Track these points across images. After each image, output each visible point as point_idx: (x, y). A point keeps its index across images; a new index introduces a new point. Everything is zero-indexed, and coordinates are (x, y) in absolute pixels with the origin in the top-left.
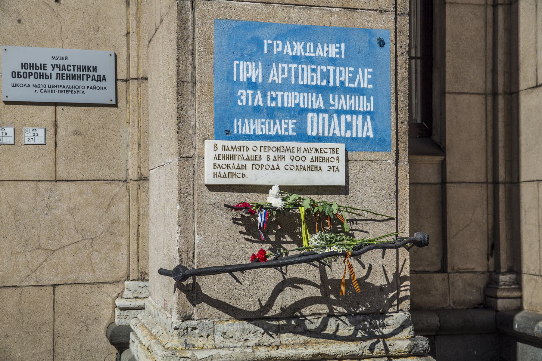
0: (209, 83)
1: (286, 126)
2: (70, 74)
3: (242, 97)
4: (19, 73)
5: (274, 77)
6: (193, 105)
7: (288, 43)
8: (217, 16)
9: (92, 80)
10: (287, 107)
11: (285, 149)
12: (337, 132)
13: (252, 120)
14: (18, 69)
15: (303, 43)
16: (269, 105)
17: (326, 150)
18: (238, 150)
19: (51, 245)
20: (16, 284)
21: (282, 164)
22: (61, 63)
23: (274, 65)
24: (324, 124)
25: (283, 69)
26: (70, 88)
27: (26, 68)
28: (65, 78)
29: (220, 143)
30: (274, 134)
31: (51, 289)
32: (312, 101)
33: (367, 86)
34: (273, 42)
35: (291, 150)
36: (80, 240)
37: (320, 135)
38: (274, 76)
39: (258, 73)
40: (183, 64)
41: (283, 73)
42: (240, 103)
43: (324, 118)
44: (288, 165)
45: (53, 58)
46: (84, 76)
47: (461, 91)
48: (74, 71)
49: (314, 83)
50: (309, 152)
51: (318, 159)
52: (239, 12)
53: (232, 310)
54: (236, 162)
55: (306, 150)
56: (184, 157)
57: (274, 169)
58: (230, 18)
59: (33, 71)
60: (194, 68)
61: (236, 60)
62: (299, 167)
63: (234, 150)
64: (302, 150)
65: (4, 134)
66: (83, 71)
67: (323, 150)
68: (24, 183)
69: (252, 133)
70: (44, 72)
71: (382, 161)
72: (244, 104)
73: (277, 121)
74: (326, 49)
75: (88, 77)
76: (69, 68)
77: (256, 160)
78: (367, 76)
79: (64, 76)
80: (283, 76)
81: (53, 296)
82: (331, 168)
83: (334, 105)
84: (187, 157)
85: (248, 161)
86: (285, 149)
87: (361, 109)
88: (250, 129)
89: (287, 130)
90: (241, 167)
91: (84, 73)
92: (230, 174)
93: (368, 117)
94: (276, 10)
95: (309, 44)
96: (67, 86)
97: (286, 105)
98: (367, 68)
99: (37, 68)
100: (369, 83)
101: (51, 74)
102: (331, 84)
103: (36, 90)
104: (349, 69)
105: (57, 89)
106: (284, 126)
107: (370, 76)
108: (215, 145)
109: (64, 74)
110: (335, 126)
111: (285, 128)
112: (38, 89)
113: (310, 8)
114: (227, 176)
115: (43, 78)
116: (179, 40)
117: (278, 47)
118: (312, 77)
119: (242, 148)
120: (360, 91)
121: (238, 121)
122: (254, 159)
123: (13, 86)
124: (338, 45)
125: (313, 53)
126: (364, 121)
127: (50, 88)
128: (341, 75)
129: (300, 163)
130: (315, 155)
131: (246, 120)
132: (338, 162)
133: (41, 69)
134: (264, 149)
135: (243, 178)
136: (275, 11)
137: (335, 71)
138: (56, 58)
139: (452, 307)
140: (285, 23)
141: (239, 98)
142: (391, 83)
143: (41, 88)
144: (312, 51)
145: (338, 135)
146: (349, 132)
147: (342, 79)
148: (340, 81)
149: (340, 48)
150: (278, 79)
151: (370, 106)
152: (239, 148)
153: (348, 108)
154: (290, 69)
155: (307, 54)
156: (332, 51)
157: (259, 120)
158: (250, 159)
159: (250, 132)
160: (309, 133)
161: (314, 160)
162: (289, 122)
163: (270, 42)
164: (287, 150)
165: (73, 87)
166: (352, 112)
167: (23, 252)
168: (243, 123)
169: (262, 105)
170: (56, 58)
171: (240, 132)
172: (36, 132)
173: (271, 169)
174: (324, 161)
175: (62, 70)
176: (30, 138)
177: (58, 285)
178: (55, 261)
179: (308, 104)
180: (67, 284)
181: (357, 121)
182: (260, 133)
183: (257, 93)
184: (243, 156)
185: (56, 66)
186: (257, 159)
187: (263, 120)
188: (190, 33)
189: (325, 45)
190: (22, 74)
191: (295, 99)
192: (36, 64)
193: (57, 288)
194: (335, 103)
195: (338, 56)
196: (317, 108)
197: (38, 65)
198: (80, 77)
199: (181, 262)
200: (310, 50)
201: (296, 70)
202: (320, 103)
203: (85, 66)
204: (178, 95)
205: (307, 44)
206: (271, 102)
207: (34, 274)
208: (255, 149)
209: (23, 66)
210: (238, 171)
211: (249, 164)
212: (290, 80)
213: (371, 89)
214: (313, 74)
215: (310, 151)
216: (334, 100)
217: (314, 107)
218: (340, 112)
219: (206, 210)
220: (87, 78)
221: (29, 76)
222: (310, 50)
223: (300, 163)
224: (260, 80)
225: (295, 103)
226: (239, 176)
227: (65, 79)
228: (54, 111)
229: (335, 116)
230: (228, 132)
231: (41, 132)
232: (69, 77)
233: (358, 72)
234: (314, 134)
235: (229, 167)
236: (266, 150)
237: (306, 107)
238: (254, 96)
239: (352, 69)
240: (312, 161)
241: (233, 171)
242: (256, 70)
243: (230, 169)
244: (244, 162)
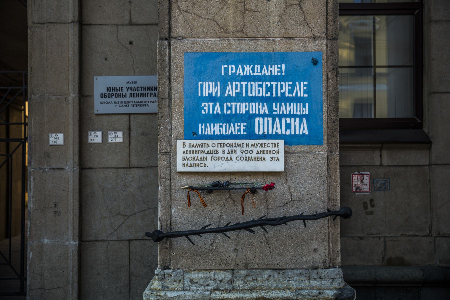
0: (180, 99)
1: (239, 128)
2: (138, 93)
4: (106, 95)
5: (229, 92)
6: (170, 115)
7: (240, 66)
8: (186, 50)
9: (154, 97)
10: (240, 113)
11: (236, 145)
12: (279, 131)
13: (212, 124)
14: (105, 91)
15: (252, 66)
16: (225, 112)
17: (269, 145)
18: (201, 146)
19: (127, 212)
20: (104, 239)
21: (234, 156)
22: (132, 85)
23: (229, 83)
24: (268, 125)
25: (236, 86)
26: (139, 102)
27: (110, 91)
28: (136, 96)
29: (187, 142)
30: (230, 134)
31: (127, 243)
32: (259, 109)
33: (303, 96)
34: (228, 67)
35: (242, 146)
36: (146, 209)
37: (265, 133)
38: (229, 91)
39: (217, 90)
40: (162, 86)
41: (236, 88)
42: (203, 112)
43: (268, 121)
44: (239, 157)
45: (128, 83)
46: (148, 94)
47: (445, 91)
48: (141, 91)
49: (260, 95)
50: (255, 147)
51: (262, 152)
52: (202, 46)
53: (198, 263)
54: (199, 156)
55: (253, 145)
56: (163, 153)
57: (228, 160)
58: (196, 51)
59: (114, 93)
60: (170, 88)
61: (200, 81)
62: (247, 158)
63: (198, 147)
64: (250, 146)
65: (96, 136)
66: (148, 91)
67: (266, 145)
68: (109, 170)
70: (122, 92)
72: (207, 112)
73: (232, 124)
74: (270, 69)
75: (151, 94)
76: (138, 89)
77: (214, 153)
78: (303, 88)
79: (135, 95)
80: (237, 91)
81: (128, 247)
82: (273, 159)
83: (276, 111)
84: (165, 152)
85: (208, 154)
86: (236, 145)
87: (298, 113)
88: (211, 131)
89: (239, 130)
90: (203, 159)
91: (148, 92)
92: (195, 164)
93: (304, 119)
94: (231, 43)
95: (256, 66)
96: (137, 102)
97: (238, 112)
98: (303, 82)
99: (117, 90)
100: (304, 93)
101: (126, 94)
102: (274, 95)
103: (116, 106)
104: (288, 83)
105: (130, 104)
106: (237, 128)
108: (184, 144)
109: (135, 93)
110: (277, 127)
111: (238, 129)
112: (118, 105)
113: (257, 40)
114: (193, 165)
115: (121, 97)
116: (159, 69)
117: (232, 69)
118: (259, 91)
119: (204, 145)
120: (297, 100)
121: (202, 126)
122: (213, 153)
123: (102, 103)
124: (279, 66)
125: (259, 73)
127: (126, 103)
128: (282, 88)
129: (249, 155)
130: (259, 149)
131: (208, 124)
132: (279, 154)
133: (119, 91)
134: (221, 145)
135: (204, 166)
136: (230, 43)
137: (277, 86)
138: (130, 83)
139: (438, 265)
140: (237, 52)
141: (203, 108)
142: (323, 92)
143: (120, 104)
144: (259, 71)
145: (280, 133)
146: (288, 131)
147: (283, 91)
148: (281, 92)
149: (281, 68)
151: (306, 111)
152: (202, 145)
153: (288, 113)
154: (241, 86)
155: (255, 74)
156: (275, 70)
157: (218, 124)
158: (210, 153)
159: (211, 133)
160: (257, 132)
161: (259, 153)
162: (241, 124)
163: (226, 66)
164: (238, 145)
165: (141, 102)
167: (109, 217)
168: (206, 127)
169: (220, 113)
170: (130, 83)
172: (116, 135)
173: (226, 160)
174: (267, 153)
175: (133, 91)
176: (113, 138)
177: (132, 240)
178: (130, 223)
179: (256, 111)
180: (138, 240)
181: (295, 123)
182: (219, 133)
183: (216, 104)
184: (204, 151)
185: (129, 88)
186: (215, 153)
187: (221, 124)
188: (167, 63)
189: (269, 66)
190: (107, 95)
191: (246, 107)
192: (116, 88)
193: (131, 242)
194: (277, 109)
195: (279, 74)
196: (263, 113)
197: (118, 88)
198: (145, 95)
199: (162, 227)
201: (247, 86)
202: (265, 110)
203: (149, 87)
204: (159, 108)
205: (254, 66)
206: (227, 111)
207: (116, 232)
208: (214, 145)
209: (108, 89)
210: (201, 162)
211: (209, 156)
213: (306, 97)
214: (259, 88)
215: (256, 146)
216: (276, 107)
217: (261, 113)
218: (281, 116)
219: (178, 190)
220: (150, 95)
221: (112, 96)
223: (249, 155)
224: (219, 95)
225: (245, 111)
226: (201, 165)
227: (135, 97)
228: (128, 119)
229: (277, 119)
230: (194, 134)
231: (120, 134)
232: (138, 95)
233: (296, 85)
234: (261, 133)
235: (194, 160)
236: (222, 146)
237: (254, 113)
238: (214, 107)
239: (290, 83)
240: (258, 153)
241: (197, 162)
242: (215, 88)
243: (195, 160)
244: (205, 156)
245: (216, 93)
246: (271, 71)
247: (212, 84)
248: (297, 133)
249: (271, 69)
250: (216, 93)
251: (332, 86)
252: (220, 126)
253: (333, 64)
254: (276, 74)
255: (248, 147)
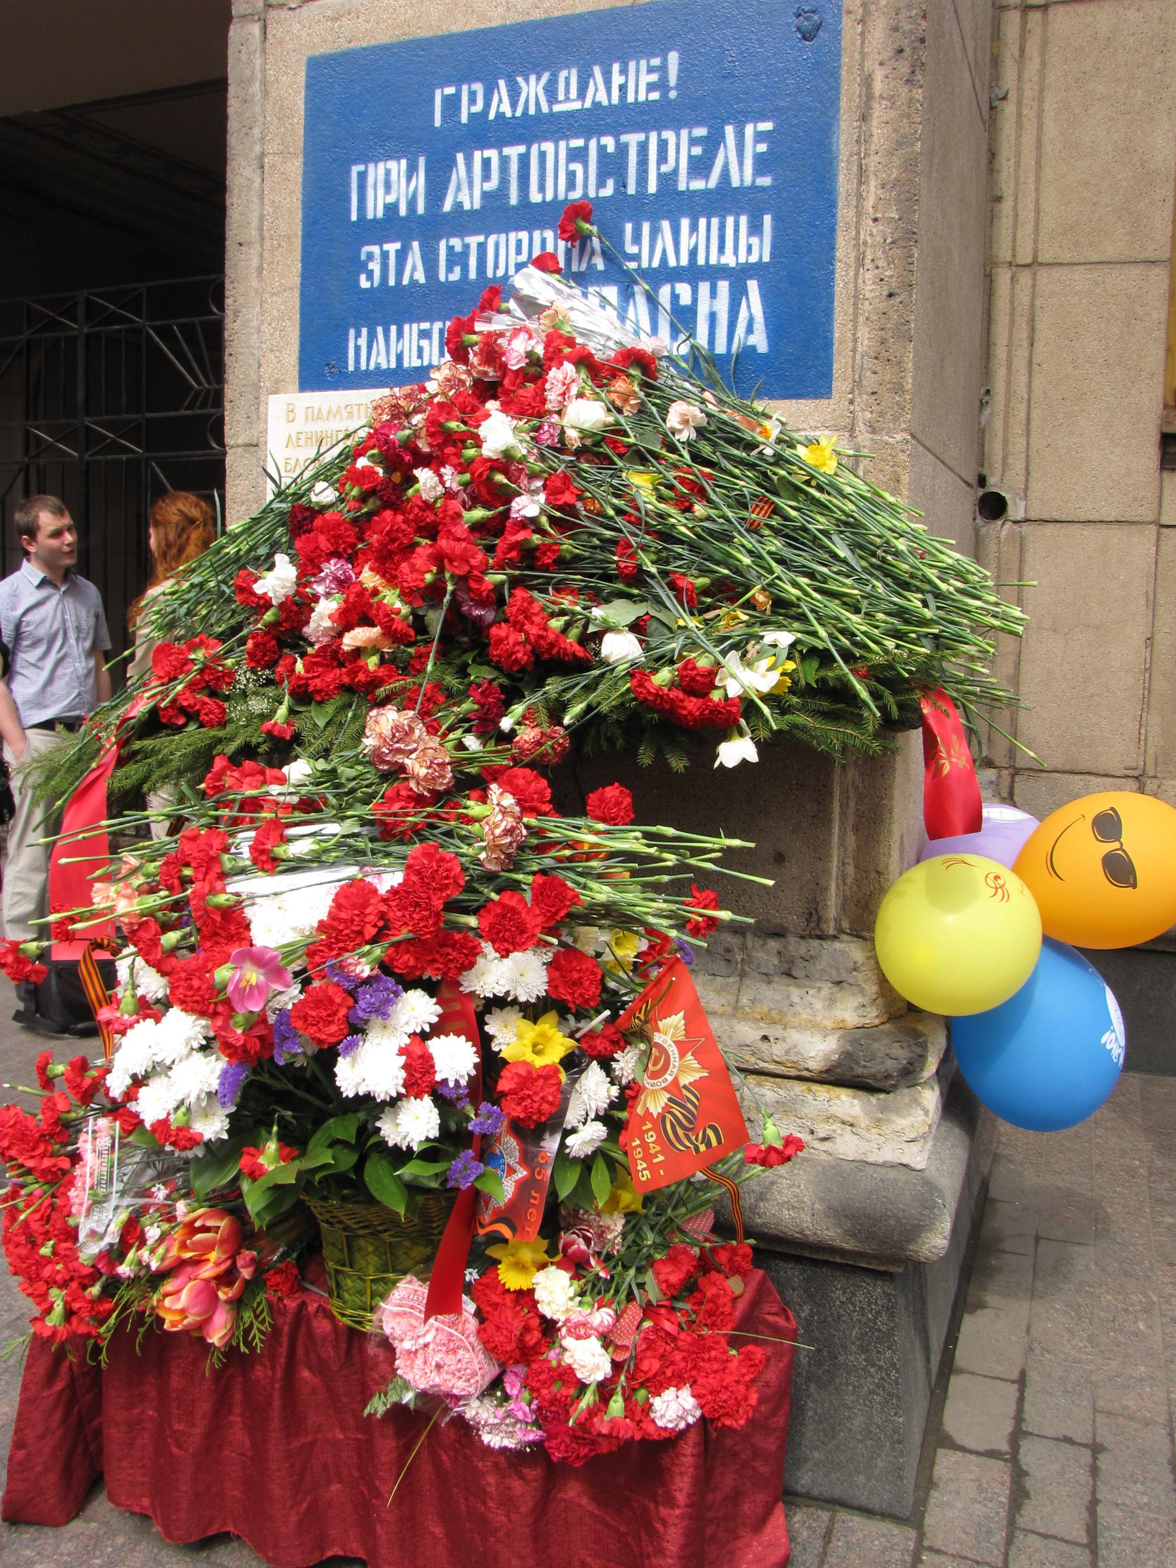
3: (371, 266)
7: (502, 83)
13: (393, 328)
15: (546, 77)
16: (442, 278)
25: (486, 163)
34: (459, 91)
38: (458, 189)
41: (486, 177)
42: (364, 284)
52: (368, 22)
61: (356, 161)
69: (393, 365)
74: (617, 80)
83: (636, 258)
87: (729, 260)
102: (631, 190)
107: (762, 148)
118: (571, 176)
121: (358, 335)
124: (656, 62)
126: (738, 295)
128: (662, 158)
137: (643, 148)
141: (362, 267)
144: (573, 93)
148: (660, 176)
149: (663, 69)
150: (471, 197)
153: (684, 261)
154: (504, 161)
155: (557, 108)
157: (415, 326)
163: (450, 90)
166: (694, 274)
169: (422, 280)
171: (363, 367)
182: (417, 363)
187: (425, 326)
189: (616, 67)
195: (655, 96)
200: (567, 91)
201: (524, 160)
206: (449, 269)
212: (507, 196)
213: (763, 189)
214: (573, 166)
222: (567, 91)
224: (421, 209)
238: (402, 256)
239: (701, 132)
242: (409, 179)
245: (412, 203)
246: (623, 88)
247: (397, 168)
248: (721, 348)
249: (622, 80)
250: (412, 203)
254: (642, 98)
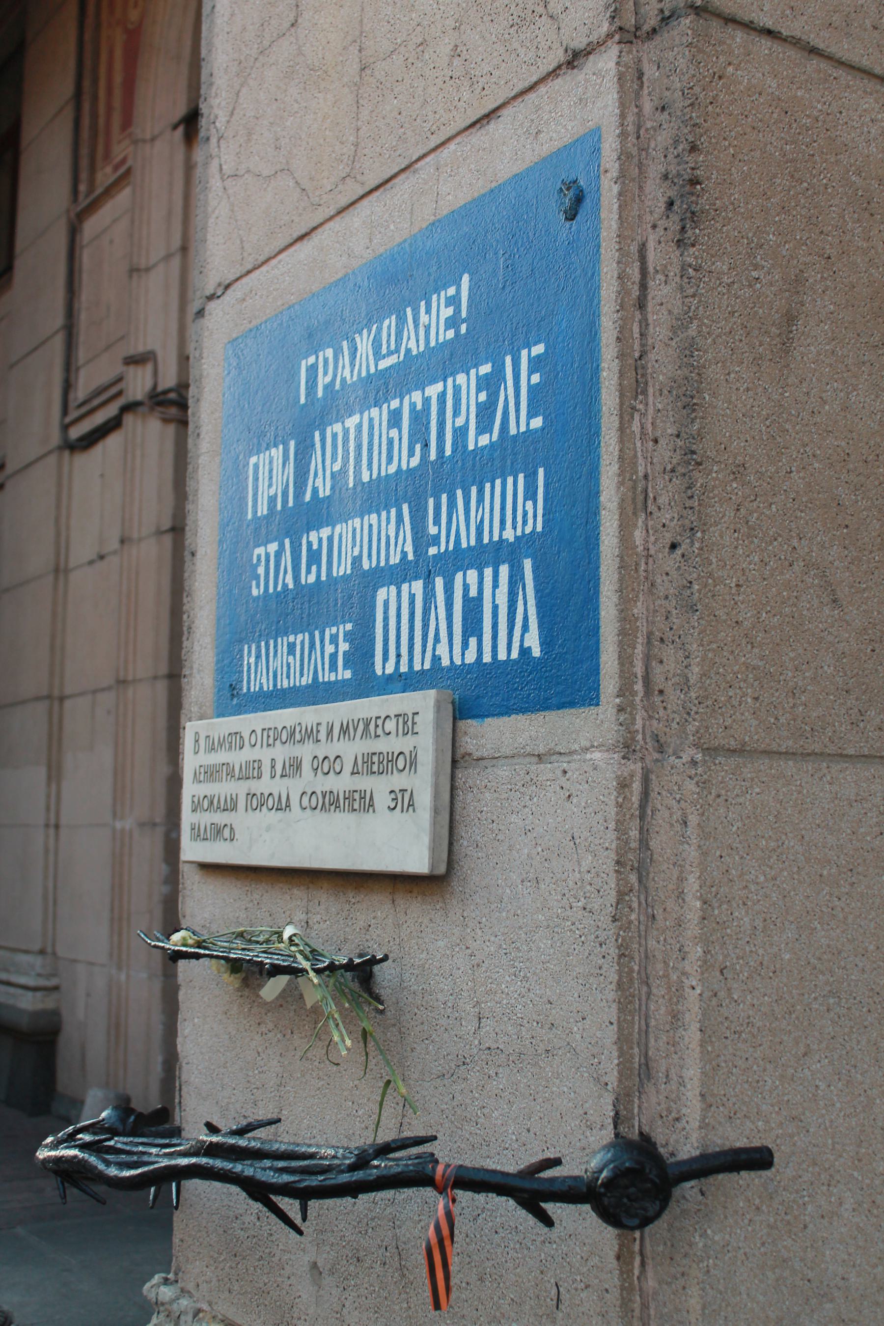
43: (412, 598)
67: (380, 722)
71: (571, 753)
132: (415, 772)
251: (663, 315)
252: (291, 648)
253: (666, 177)
255: (332, 740)
